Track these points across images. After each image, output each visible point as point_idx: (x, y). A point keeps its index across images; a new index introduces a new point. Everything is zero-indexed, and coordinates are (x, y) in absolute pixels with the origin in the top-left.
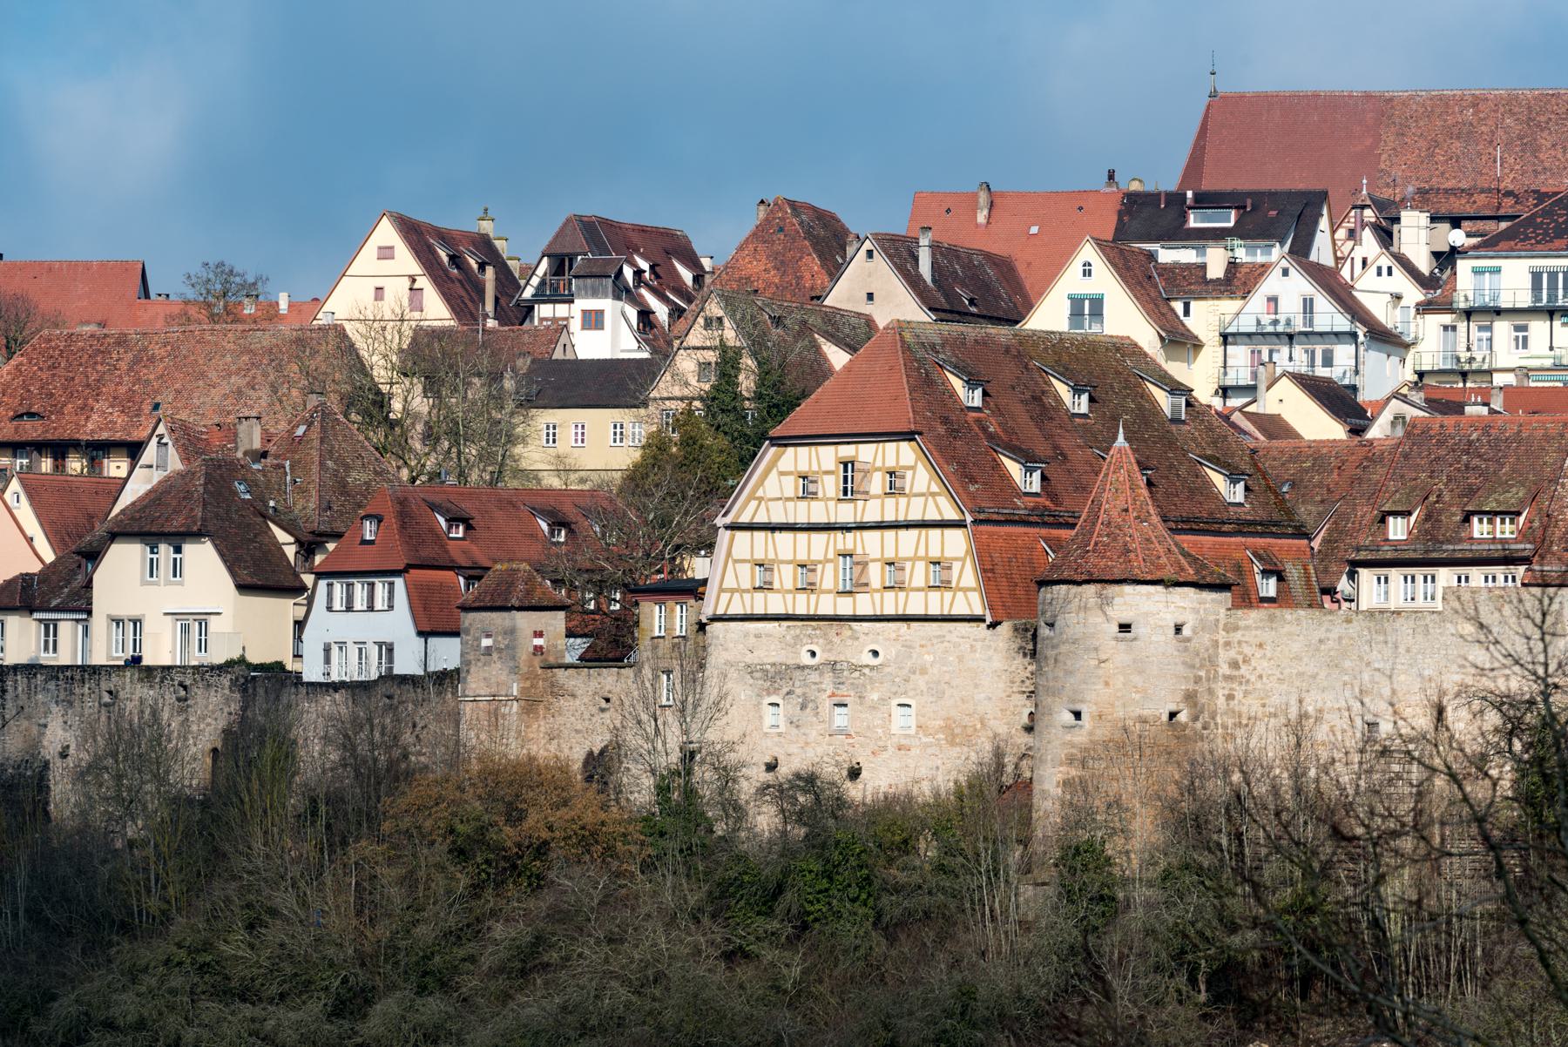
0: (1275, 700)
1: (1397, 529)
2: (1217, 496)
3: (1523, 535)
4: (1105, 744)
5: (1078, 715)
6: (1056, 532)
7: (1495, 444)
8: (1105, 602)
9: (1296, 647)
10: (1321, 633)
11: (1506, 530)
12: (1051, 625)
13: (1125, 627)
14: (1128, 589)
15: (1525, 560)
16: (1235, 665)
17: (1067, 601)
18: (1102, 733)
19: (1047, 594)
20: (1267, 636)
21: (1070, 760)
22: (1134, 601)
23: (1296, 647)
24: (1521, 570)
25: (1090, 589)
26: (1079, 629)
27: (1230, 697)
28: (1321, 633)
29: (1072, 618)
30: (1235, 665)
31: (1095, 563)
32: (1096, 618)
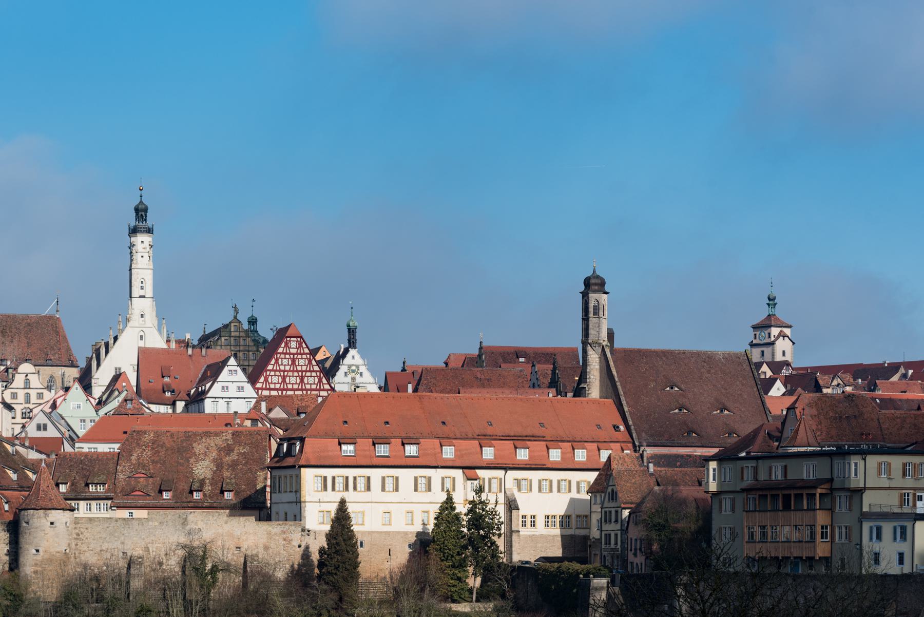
0: (92, 546)
1: (63, 488)
2: (30, 479)
3: (108, 491)
4: (47, 560)
5: (37, 551)
6: (4, 492)
7: (90, 461)
8: (46, 515)
9: (99, 529)
10: (107, 525)
11: (100, 489)
12: (27, 523)
13: (52, 523)
14: (53, 511)
15: (111, 499)
16: (78, 535)
17: (33, 515)
18: (46, 556)
19: (23, 512)
20: (89, 526)
21: (36, 565)
22: (55, 515)
23: (99, 529)
24: (109, 502)
25: (41, 512)
26: (38, 524)
27: (77, 545)
28: (107, 525)
29: (35, 520)
30: (78, 535)
31: (41, 503)
32: (43, 521)
